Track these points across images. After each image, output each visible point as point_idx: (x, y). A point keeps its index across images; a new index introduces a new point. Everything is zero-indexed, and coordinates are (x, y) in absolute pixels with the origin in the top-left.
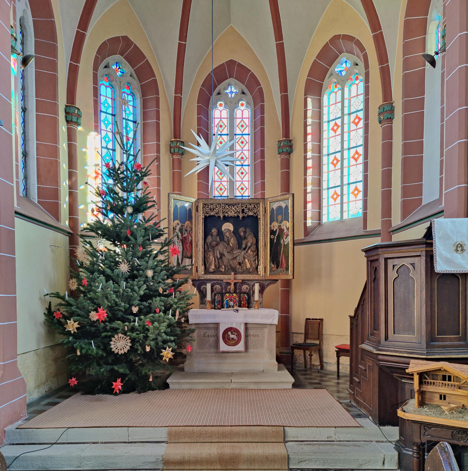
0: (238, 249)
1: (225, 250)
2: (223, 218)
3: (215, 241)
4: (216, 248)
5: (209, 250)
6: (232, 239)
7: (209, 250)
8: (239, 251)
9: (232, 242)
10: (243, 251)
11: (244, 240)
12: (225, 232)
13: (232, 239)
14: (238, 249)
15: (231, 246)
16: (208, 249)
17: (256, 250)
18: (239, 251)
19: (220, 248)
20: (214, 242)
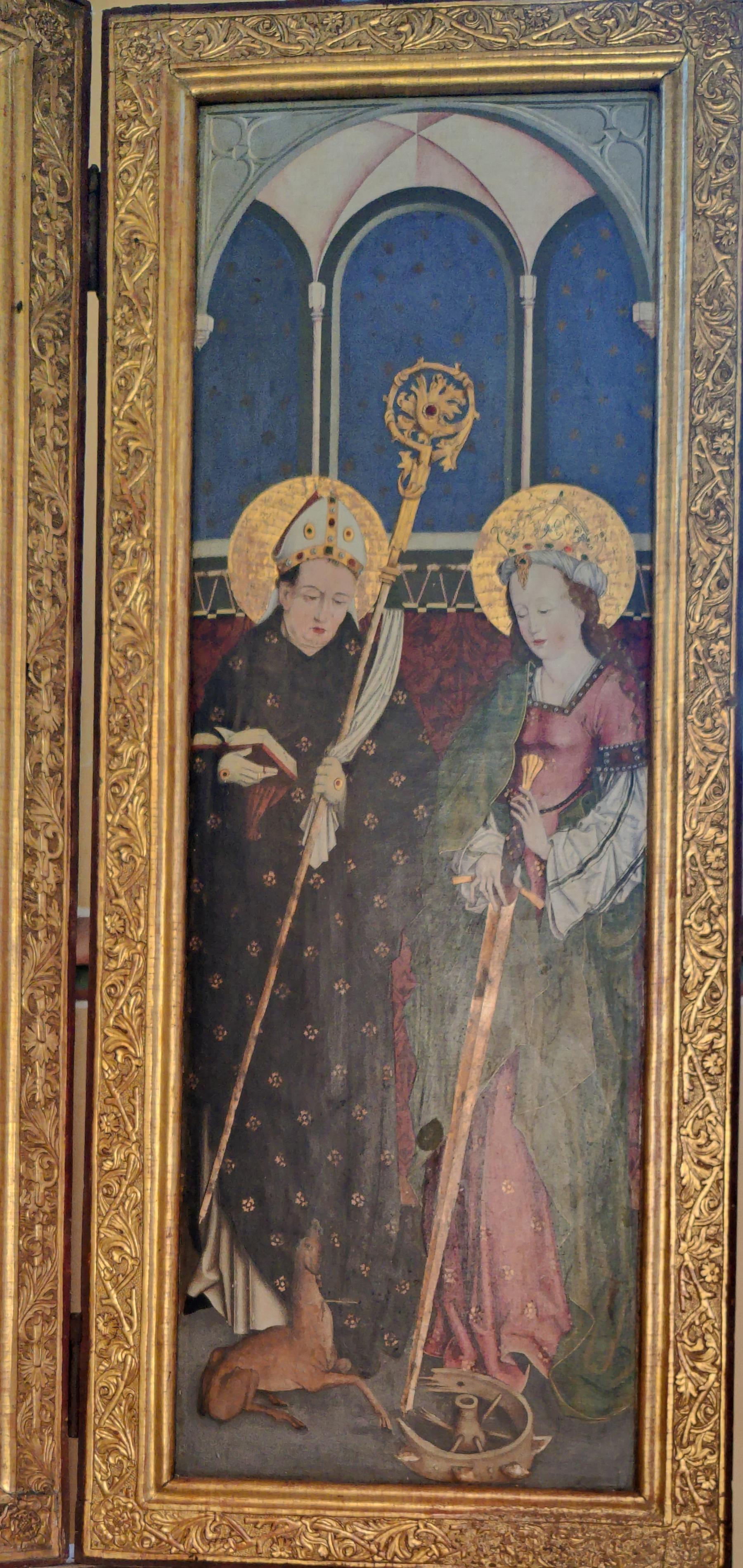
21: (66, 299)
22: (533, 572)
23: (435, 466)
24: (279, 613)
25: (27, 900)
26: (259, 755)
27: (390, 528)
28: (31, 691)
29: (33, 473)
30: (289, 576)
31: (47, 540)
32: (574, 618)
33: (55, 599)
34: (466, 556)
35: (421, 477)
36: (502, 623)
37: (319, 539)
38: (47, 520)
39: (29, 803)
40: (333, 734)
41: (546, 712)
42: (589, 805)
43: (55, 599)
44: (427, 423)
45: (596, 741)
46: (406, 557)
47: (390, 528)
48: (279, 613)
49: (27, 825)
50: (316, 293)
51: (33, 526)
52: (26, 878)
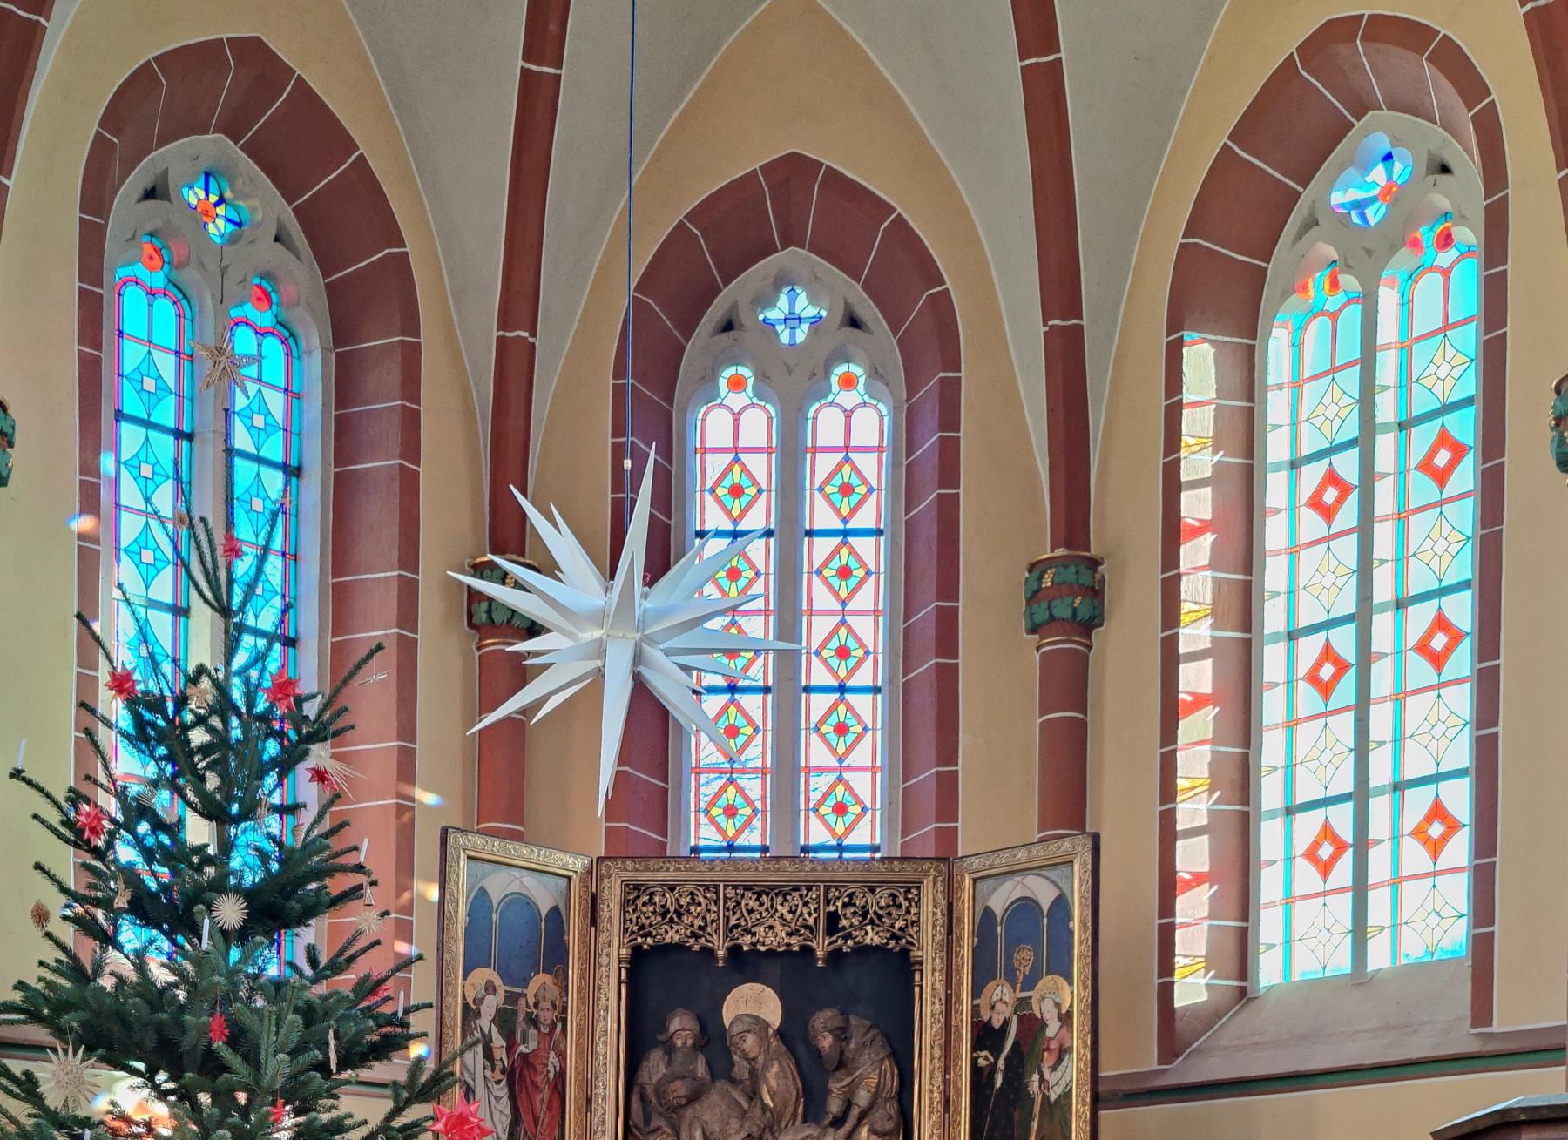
0: (805, 1121)
1: (735, 1124)
2: (726, 960)
3: (683, 1078)
4: (689, 1113)
5: (653, 1125)
6: (775, 1068)
7: (653, 1125)
8: (808, 1132)
9: (773, 1083)
10: (831, 1130)
11: (839, 1074)
12: (735, 1030)
13: (775, 1068)
14: (805, 1121)
15: (764, 1107)
16: (647, 1120)
17: (897, 1127)
18: (808, 1132)
19: (707, 1117)
20: (678, 1084)
21: (943, 940)
22: (1046, 1000)
23: (1024, 973)
24: (990, 1019)
25: (931, 1104)
26: (986, 1058)
27: (1014, 992)
28: (932, 1047)
29: (933, 989)
30: (993, 1008)
31: (937, 1006)
32: (1055, 1012)
33: (939, 1021)
34: (1031, 997)
35: (1021, 977)
36: (1040, 1017)
37: (999, 997)
38: (937, 1000)
39: (931, 1078)
40: (1001, 1051)
41: (1050, 1039)
42: (1059, 1064)
43: (939, 1021)
44: (1022, 962)
45: (1061, 1046)
46: (1018, 1000)
47: (1014, 992)
48: (990, 1019)
49: (931, 1084)
50: (999, 928)
51: (933, 1003)
52: (931, 1099)
